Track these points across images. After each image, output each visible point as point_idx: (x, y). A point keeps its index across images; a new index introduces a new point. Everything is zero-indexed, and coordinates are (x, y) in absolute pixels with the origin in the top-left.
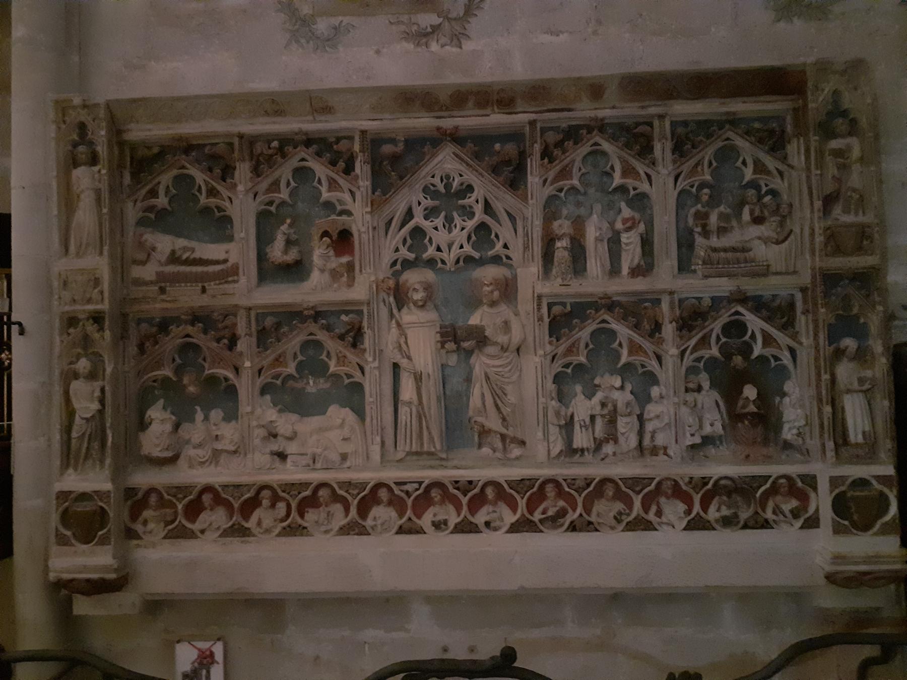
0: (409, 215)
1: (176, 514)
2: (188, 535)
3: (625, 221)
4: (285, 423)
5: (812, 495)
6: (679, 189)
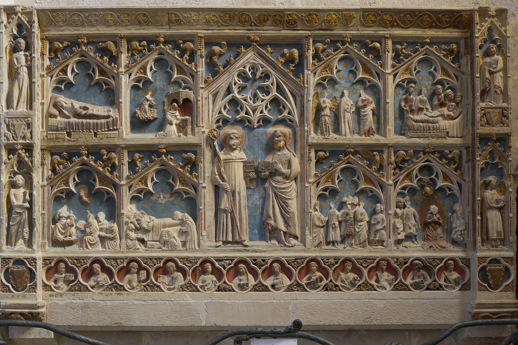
0: (229, 91)
1: (76, 277)
2: (81, 288)
3: (363, 101)
4: (147, 220)
5: (467, 270)
6: (396, 83)
